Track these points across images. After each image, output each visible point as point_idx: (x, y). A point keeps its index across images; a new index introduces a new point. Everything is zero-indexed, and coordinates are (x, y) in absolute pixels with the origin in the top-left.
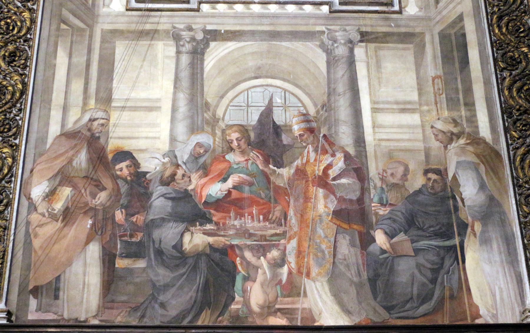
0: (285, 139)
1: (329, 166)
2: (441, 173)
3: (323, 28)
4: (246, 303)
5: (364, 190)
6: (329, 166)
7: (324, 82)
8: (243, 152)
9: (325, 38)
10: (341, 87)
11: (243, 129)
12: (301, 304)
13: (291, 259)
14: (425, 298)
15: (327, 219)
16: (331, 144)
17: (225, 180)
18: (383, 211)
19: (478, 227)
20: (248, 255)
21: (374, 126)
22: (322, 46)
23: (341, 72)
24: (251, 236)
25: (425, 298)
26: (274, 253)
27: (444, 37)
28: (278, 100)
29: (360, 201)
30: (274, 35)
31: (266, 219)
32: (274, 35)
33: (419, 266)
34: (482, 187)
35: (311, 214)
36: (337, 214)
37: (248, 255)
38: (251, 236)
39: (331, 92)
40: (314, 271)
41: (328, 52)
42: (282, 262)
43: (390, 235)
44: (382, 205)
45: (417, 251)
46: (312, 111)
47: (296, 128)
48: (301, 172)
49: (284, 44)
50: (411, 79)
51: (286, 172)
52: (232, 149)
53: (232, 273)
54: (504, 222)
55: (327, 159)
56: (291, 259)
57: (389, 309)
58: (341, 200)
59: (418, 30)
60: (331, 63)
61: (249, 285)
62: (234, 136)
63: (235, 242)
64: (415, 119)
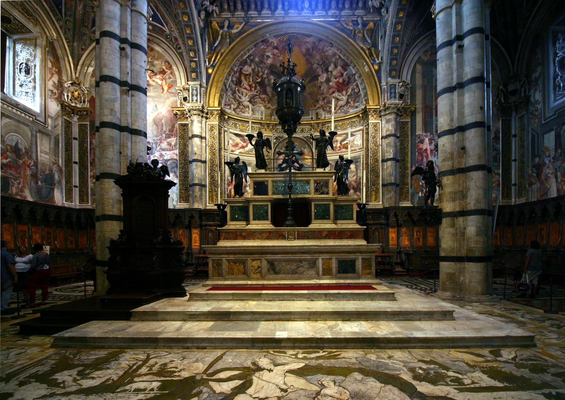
0: (21, 153)
1: (30, 163)
2: (52, 171)
3: (29, 124)
4: (12, 191)
5: (37, 171)
6: (30, 163)
7: (30, 140)
8: (11, 153)
9: (31, 127)
10: (34, 143)
11: (11, 146)
12: (23, 194)
13: (22, 183)
14: (47, 197)
15: (29, 176)
16: (31, 157)
17: (6, 159)
18: (41, 177)
19: (57, 185)
20: (12, 180)
21: (40, 156)
22: (30, 130)
23: (34, 139)
24: (13, 176)
25: (47, 197)
26: (18, 181)
27: (55, 138)
28: (19, 141)
29: (36, 173)
30: (19, 121)
31: (16, 172)
32: (19, 121)
33: (46, 191)
34: (59, 177)
35: (26, 174)
36: (32, 175)
37: (12, 180)
38: (13, 176)
39: (32, 144)
40: (27, 187)
41: (32, 132)
42: (19, 184)
43: (42, 183)
44: (41, 175)
45: (46, 187)
46: (27, 147)
47: (23, 150)
48: (24, 163)
49: (21, 125)
50: (48, 146)
51: (21, 162)
52: (8, 151)
53: (9, 184)
54: (61, 185)
55: (30, 161)
56: (22, 183)
57: (40, 198)
58: (32, 172)
59: (50, 134)
60: (32, 135)
61: (13, 188)
62: (9, 148)
63: (9, 176)
64: (47, 157)
